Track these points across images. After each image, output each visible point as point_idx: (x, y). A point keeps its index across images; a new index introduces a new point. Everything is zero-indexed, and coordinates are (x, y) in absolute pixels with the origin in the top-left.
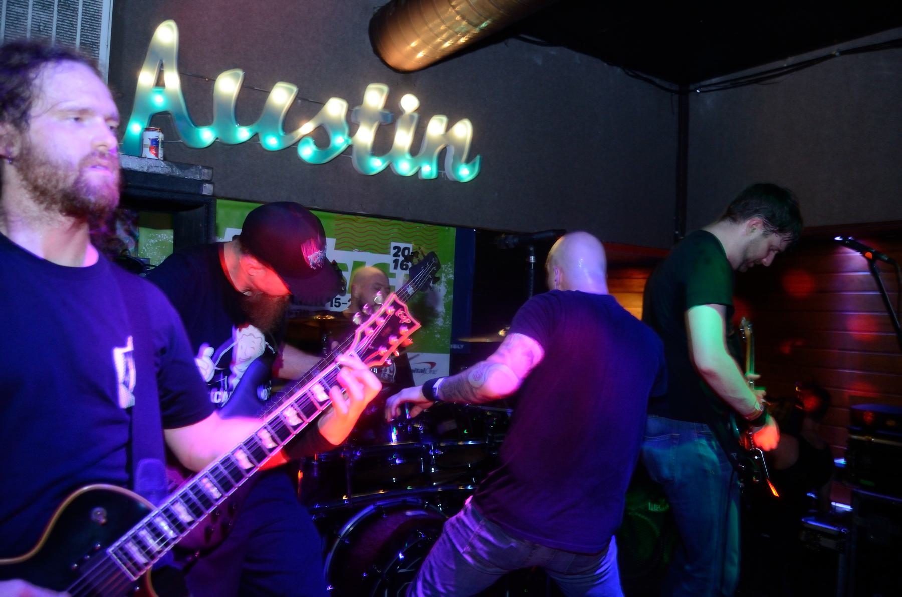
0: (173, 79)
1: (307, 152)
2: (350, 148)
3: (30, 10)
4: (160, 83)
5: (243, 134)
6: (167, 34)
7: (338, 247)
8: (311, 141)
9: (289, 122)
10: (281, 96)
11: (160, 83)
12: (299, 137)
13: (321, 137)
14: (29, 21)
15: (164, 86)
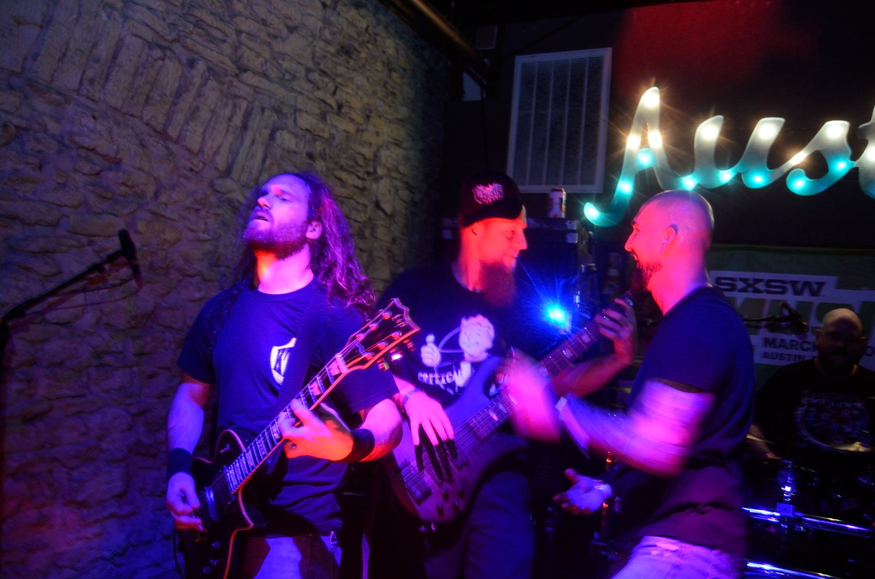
0: (657, 139)
1: (799, 185)
2: (854, 173)
3: (550, 110)
4: (644, 144)
5: (725, 176)
6: (651, 99)
7: (840, 286)
8: (803, 171)
9: (774, 157)
10: (767, 131)
11: (644, 144)
12: (786, 170)
13: (818, 167)
14: (549, 119)
15: (648, 147)
